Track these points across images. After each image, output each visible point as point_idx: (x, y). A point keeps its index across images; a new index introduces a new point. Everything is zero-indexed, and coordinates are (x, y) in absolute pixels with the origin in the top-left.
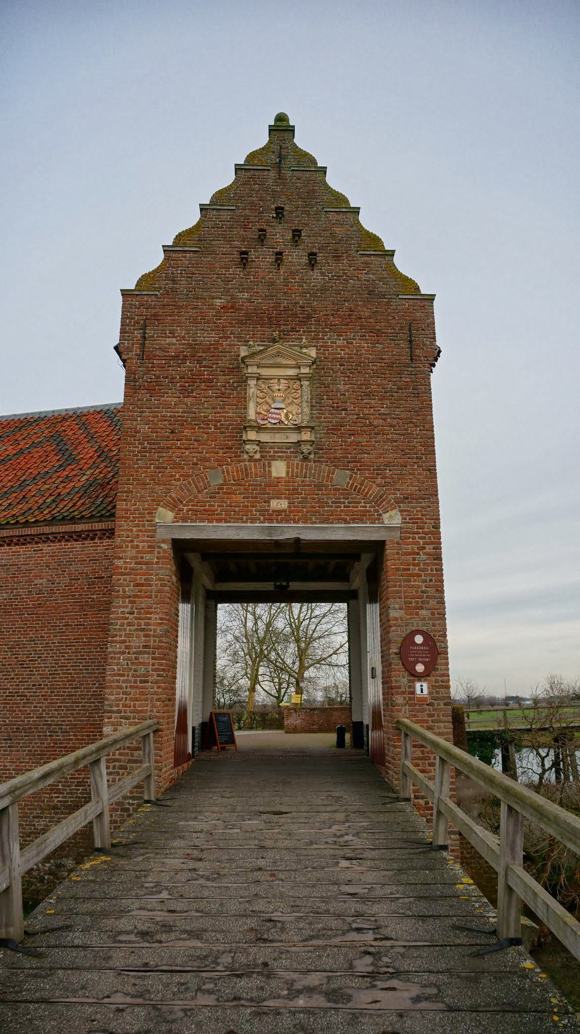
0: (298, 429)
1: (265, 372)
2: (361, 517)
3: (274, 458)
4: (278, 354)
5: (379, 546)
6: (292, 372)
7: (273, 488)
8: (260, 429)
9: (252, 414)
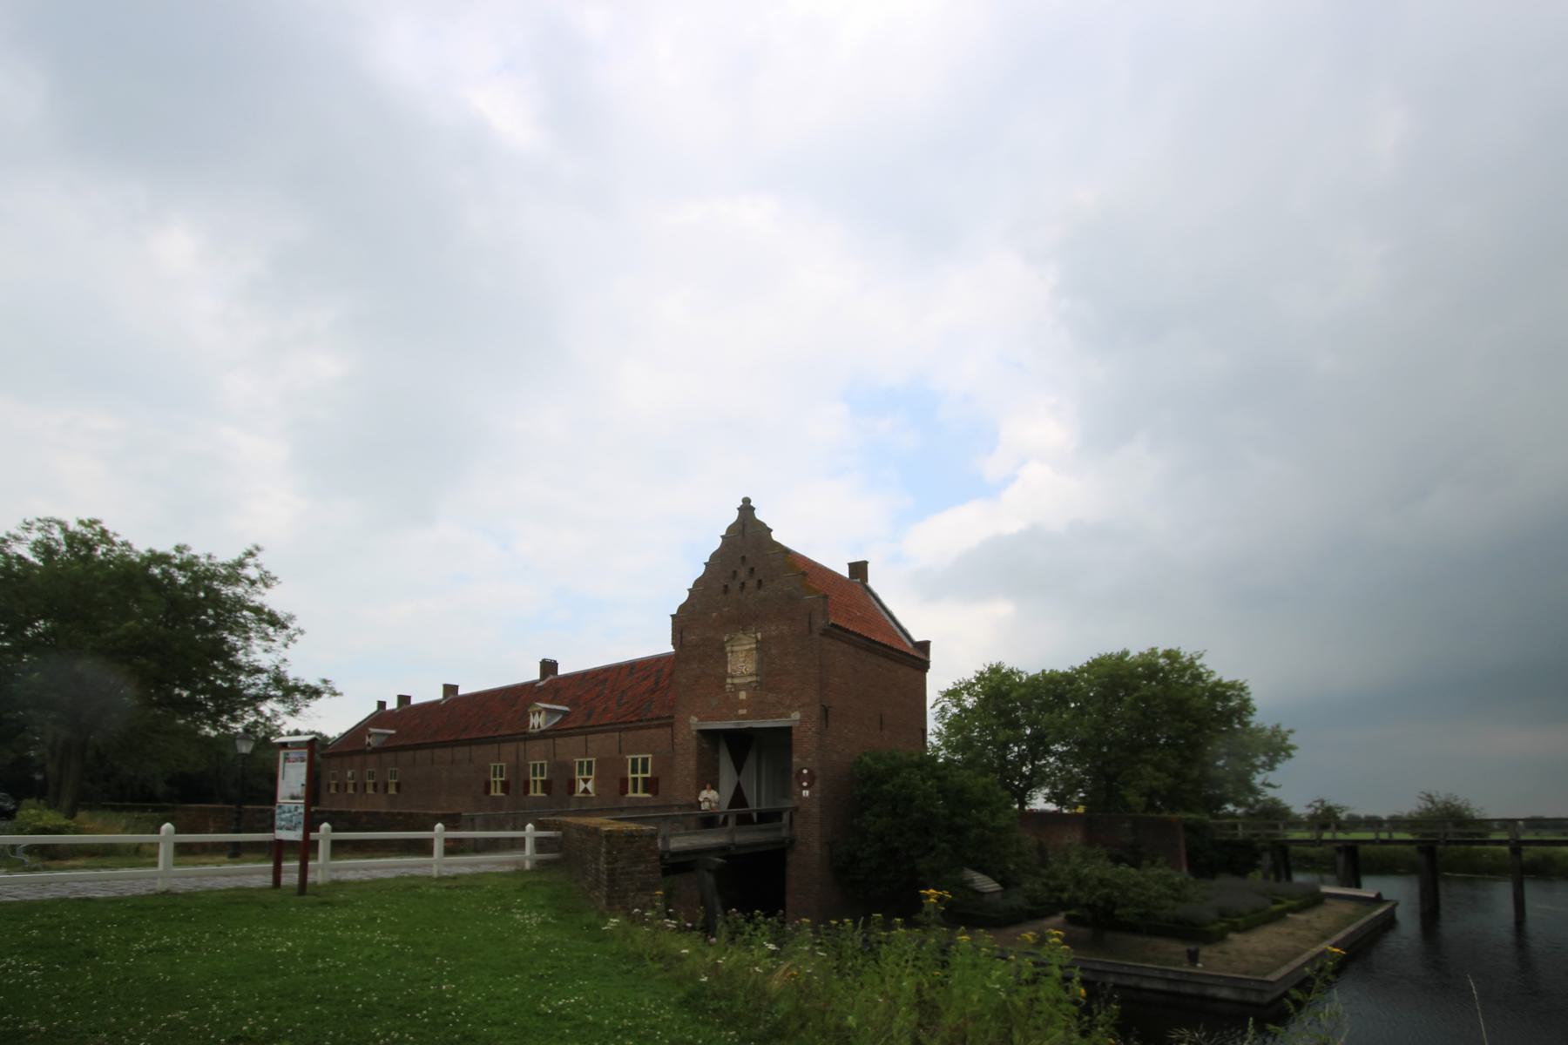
0: (751, 675)
1: (735, 649)
2: (780, 716)
3: (740, 690)
4: (740, 639)
5: (787, 731)
6: (748, 647)
7: (741, 704)
8: (733, 677)
9: (729, 671)
